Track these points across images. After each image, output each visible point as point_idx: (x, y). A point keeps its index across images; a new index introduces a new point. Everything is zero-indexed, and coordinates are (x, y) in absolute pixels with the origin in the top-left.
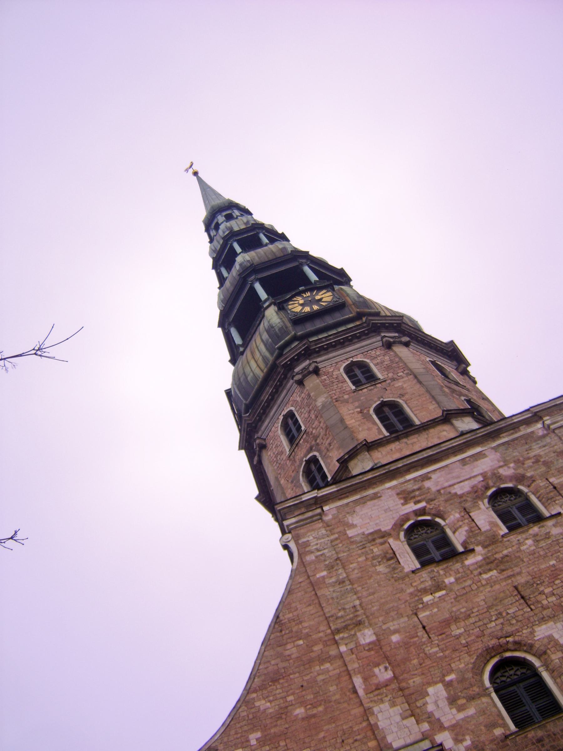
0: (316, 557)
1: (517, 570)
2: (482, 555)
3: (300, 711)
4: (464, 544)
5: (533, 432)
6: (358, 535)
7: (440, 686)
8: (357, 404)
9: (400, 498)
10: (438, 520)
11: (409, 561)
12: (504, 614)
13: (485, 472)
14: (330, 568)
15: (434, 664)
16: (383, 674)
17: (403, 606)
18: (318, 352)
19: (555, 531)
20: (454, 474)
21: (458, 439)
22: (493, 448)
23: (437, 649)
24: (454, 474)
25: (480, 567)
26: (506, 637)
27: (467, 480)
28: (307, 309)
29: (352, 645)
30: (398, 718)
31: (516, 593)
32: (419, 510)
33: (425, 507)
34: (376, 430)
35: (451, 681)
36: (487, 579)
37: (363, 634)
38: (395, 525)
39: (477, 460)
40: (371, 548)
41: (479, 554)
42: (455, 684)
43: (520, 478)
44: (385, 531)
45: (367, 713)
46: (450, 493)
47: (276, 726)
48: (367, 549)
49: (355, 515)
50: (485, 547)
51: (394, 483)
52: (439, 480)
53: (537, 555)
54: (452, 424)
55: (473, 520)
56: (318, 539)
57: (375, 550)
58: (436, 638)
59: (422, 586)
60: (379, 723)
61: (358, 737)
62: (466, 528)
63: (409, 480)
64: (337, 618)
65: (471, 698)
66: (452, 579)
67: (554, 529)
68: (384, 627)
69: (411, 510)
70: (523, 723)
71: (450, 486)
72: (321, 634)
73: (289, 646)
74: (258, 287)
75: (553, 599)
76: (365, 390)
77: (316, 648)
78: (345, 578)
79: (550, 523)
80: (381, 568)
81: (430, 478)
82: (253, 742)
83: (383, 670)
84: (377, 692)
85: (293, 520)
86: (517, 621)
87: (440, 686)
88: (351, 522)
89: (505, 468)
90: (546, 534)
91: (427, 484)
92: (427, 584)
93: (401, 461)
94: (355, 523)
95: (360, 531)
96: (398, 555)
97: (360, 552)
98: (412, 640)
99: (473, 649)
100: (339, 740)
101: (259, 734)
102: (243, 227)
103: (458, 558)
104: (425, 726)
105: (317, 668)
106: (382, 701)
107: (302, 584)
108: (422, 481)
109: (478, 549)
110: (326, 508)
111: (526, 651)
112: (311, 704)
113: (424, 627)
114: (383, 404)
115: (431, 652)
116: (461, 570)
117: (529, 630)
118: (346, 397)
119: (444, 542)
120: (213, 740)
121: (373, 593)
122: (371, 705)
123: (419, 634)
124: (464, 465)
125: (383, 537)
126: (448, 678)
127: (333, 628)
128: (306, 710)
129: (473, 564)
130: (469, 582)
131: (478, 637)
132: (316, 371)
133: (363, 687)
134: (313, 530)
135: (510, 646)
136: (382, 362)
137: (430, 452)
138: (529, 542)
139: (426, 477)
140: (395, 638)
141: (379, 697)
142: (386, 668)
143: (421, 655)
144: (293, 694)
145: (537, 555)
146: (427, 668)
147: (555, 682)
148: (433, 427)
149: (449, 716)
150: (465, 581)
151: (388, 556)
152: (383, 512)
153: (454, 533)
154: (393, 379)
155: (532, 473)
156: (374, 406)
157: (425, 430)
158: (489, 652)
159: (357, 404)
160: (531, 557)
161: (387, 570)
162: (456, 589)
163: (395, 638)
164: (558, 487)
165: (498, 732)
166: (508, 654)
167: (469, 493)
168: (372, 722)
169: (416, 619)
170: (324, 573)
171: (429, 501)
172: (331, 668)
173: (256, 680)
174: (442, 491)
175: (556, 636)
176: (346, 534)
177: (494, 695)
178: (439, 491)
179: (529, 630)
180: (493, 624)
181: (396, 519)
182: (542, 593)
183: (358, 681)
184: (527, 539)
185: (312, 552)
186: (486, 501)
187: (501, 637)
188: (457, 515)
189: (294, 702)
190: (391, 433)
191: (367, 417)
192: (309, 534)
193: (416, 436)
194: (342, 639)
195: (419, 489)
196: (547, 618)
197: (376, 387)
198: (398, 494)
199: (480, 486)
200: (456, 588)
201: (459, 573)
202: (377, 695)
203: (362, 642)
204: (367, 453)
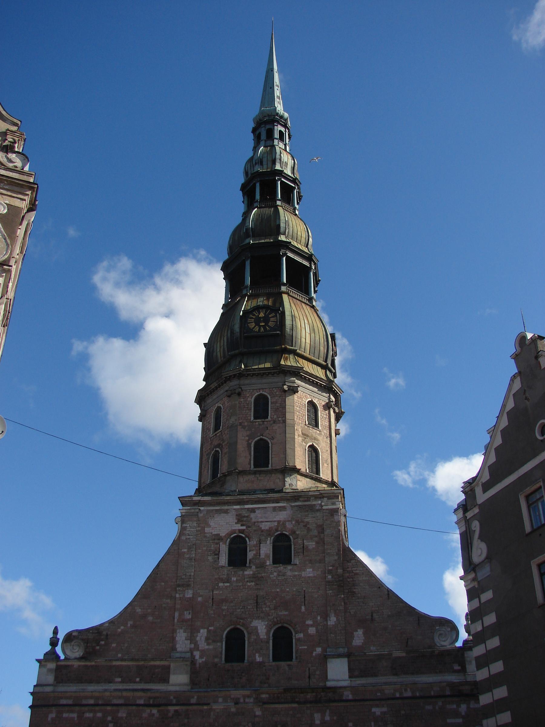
3: (150, 618)
4: (250, 560)
5: (315, 505)
7: (206, 630)
8: (248, 433)
10: (247, 539)
11: (224, 560)
13: (280, 521)
14: (189, 548)
16: (188, 616)
19: (289, 573)
22: (291, 506)
25: (249, 578)
27: (270, 521)
29: (181, 596)
30: (184, 638)
31: (256, 599)
35: (211, 630)
36: (249, 586)
39: (280, 511)
43: (293, 532)
45: (174, 631)
50: (257, 567)
54: (284, 476)
56: (191, 527)
57: (212, 546)
62: (254, 552)
63: (246, 509)
64: (182, 578)
65: (214, 641)
66: (235, 579)
68: (198, 591)
69: (237, 528)
70: (228, 659)
74: (248, 263)
75: (267, 609)
76: (257, 423)
80: (210, 558)
81: (255, 512)
82: (129, 625)
87: (206, 630)
91: (252, 515)
97: (206, 544)
104: (193, 646)
106: (182, 629)
108: (251, 512)
110: (202, 508)
113: (213, 599)
114: (261, 439)
118: (246, 424)
125: (219, 539)
126: (210, 628)
129: (247, 575)
130: (241, 584)
132: (239, 394)
135: (241, 624)
136: (276, 402)
138: (275, 574)
139: (253, 510)
140: (200, 599)
147: (248, 648)
149: (203, 645)
151: (217, 552)
152: (225, 524)
154: (274, 422)
156: (256, 439)
161: (212, 561)
163: (200, 599)
164: (305, 547)
165: (216, 660)
166: (239, 626)
167: (267, 530)
170: (186, 550)
171: (248, 527)
174: (256, 524)
175: (259, 627)
177: (224, 643)
178: (255, 522)
180: (239, 610)
183: (177, 614)
186: (272, 538)
188: (255, 543)
191: (249, 446)
194: (179, 590)
195: (247, 517)
203: (186, 596)
204: (236, 477)
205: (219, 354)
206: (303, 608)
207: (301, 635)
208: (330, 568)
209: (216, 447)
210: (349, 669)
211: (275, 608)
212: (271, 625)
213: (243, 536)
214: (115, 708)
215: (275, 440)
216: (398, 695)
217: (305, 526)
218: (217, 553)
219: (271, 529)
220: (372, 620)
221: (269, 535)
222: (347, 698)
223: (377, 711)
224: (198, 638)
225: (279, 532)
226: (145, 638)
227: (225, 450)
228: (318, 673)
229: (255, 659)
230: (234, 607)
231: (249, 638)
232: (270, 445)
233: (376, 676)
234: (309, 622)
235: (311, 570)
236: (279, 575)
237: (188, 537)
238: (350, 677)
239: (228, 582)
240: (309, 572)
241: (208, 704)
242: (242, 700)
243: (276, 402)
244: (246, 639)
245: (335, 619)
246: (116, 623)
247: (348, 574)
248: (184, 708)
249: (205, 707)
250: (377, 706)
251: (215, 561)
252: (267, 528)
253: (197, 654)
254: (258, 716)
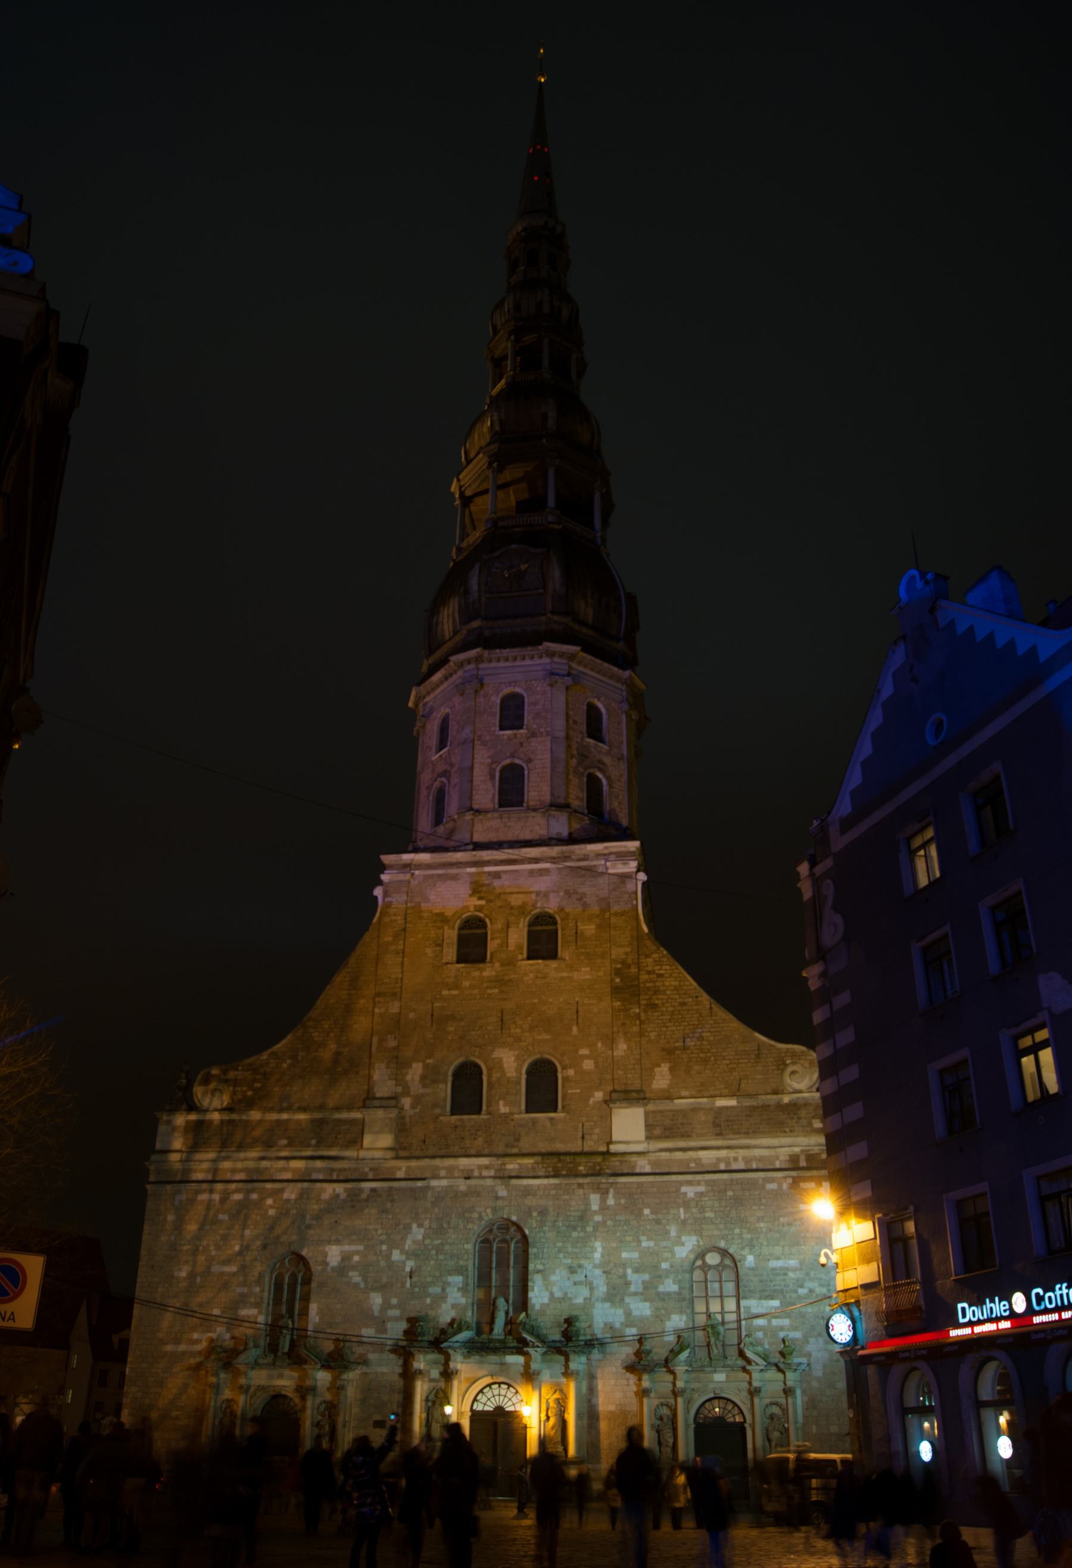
4: (492, 954)
7: (421, 1064)
10: (487, 921)
11: (450, 953)
16: (392, 1043)
22: (559, 869)
25: (490, 981)
29: (383, 1010)
39: (541, 875)
50: (502, 965)
62: (498, 941)
75: (518, 1031)
81: (500, 878)
87: (421, 1064)
91: (496, 883)
103: (481, 965)
104: (400, 1089)
118: (488, 738)
119: (483, 941)
125: (443, 921)
126: (428, 1061)
136: (536, 703)
138: (532, 975)
139: (497, 875)
140: (412, 1015)
149: (416, 1088)
151: (439, 942)
154: (533, 735)
163: (412, 1015)
171: (489, 901)
183: (375, 1040)
186: (528, 919)
188: (500, 926)
195: (488, 885)
198: (471, 883)
205: (446, 626)
206: (575, 1029)
207: (571, 1072)
208: (619, 966)
209: (440, 776)
210: (646, 1126)
211: (532, 1028)
214: (278, 1185)
216: (722, 1167)
217: (580, 899)
218: (439, 944)
220: (685, 1048)
221: (523, 913)
222: (642, 1171)
223: (690, 1191)
224: (409, 1078)
227: (455, 780)
228: (597, 1131)
229: (499, 1109)
231: (489, 1077)
232: (526, 772)
233: (689, 1136)
234: (584, 1051)
236: (537, 977)
238: (648, 1138)
239: (456, 986)
240: (584, 974)
241: (424, 1179)
242: (476, 1174)
243: (536, 703)
244: (485, 1078)
245: (625, 1047)
247: (646, 977)
248: (385, 1184)
249: (419, 1184)
250: (690, 1183)
252: (519, 903)
253: (406, 1102)
254: (503, 1198)
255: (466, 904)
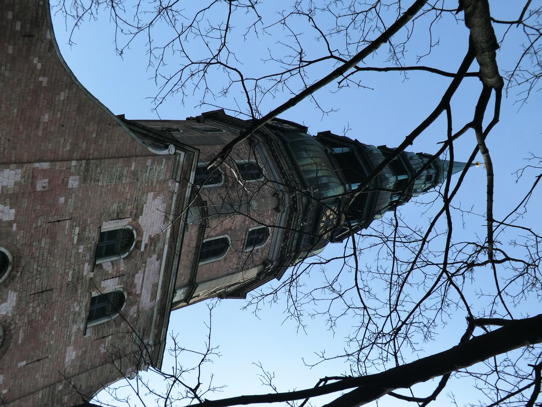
0: (147, 166)
1: (63, 295)
2: (86, 276)
3: (46, 118)
5: (149, 336)
6: (147, 200)
7: (13, 218)
8: (238, 228)
9: (155, 236)
12: (38, 276)
14: (134, 173)
15: (29, 219)
16: (41, 184)
17: (81, 212)
18: (290, 215)
20: (151, 276)
21: (173, 288)
22: (154, 307)
23: (39, 224)
24: (151, 276)
25: (79, 272)
26: (21, 272)
28: (324, 219)
29: (73, 170)
30: (5, 184)
31: (48, 288)
32: (141, 246)
33: (140, 250)
34: (213, 233)
35: (12, 227)
37: (77, 180)
38: (140, 226)
39: (152, 294)
40: (133, 205)
41: (88, 274)
42: (9, 228)
44: (138, 218)
45: (20, 163)
46: (140, 269)
47: (44, 99)
48: (133, 202)
49: (161, 202)
50: (91, 279)
51: (168, 235)
52: (153, 265)
53: (66, 310)
54: (186, 286)
55: (113, 278)
56: (159, 172)
57: (130, 207)
58: (47, 227)
59: (87, 230)
60: (8, 170)
61: (6, 152)
63: (164, 246)
67: (77, 327)
68: (74, 195)
71: (144, 271)
72: (92, 151)
73: (96, 126)
75: (30, 310)
77: (84, 144)
78: (122, 181)
79: (82, 326)
80: (115, 206)
81: (157, 260)
82: (41, 79)
83: (44, 185)
84: (31, 175)
85: (181, 160)
86: (28, 283)
88: (158, 197)
89: (136, 311)
90: (76, 322)
91: (155, 257)
92: (87, 233)
93: (180, 246)
94: (156, 200)
95: (148, 201)
96: (117, 221)
97: (134, 196)
98: (54, 210)
99: (26, 248)
100: (11, 138)
101: (44, 84)
102: (415, 187)
105: (70, 141)
107: (134, 150)
108: (158, 254)
109: (92, 275)
110: (177, 184)
111: (5, 281)
112: (47, 128)
113: (59, 221)
114: (227, 245)
115: (40, 220)
116: (84, 258)
117: (18, 288)
120: (57, 51)
121: (101, 196)
122: (24, 169)
123: (56, 216)
124: (153, 285)
125: (136, 215)
126: (15, 225)
127: (92, 161)
128: (44, 123)
129: (83, 267)
130: (73, 260)
131: (33, 254)
132: (277, 209)
133: (40, 168)
134: (167, 171)
135: (15, 273)
137: (175, 267)
138: (77, 309)
139: (160, 257)
140: (62, 200)
141: (26, 176)
142: (44, 187)
143: (41, 213)
144: (61, 118)
145: (66, 310)
146: (30, 214)
148: (191, 273)
150: (75, 258)
151: (120, 214)
152: (153, 221)
153: (112, 262)
155: (122, 326)
156: (229, 239)
157: (193, 267)
158: (18, 257)
159: (238, 228)
160: (66, 307)
161: (111, 210)
162: (73, 251)
163: (62, 200)
164: (103, 340)
166: (10, 268)
167: (133, 281)
168: (11, 166)
169: (67, 218)
170: (133, 168)
172: (65, 150)
173: (84, 95)
174: (144, 265)
176: (152, 191)
178: (145, 263)
179: (18, 288)
180: (35, 267)
181: (143, 228)
182: (39, 305)
183: (46, 165)
184: (80, 308)
185: (152, 165)
186: (121, 290)
187: (23, 269)
188: (122, 269)
189: (55, 116)
190: (203, 244)
192: (166, 167)
193: (192, 260)
194: (81, 165)
195: (154, 250)
196: (19, 302)
197: (241, 245)
199: (134, 290)
200: (73, 252)
201: (83, 257)
202: (29, 176)
203: (71, 178)
206: (24, 363)
212: (5, 322)
213: (132, 249)
215: (222, 263)
219: (133, 285)
225: (126, 297)
226: (15, 111)
230: (41, 259)
235: (74, 357)
237: (149, 169)
246: (49, 54)
251: (109, 215)
255: (145, 233)
